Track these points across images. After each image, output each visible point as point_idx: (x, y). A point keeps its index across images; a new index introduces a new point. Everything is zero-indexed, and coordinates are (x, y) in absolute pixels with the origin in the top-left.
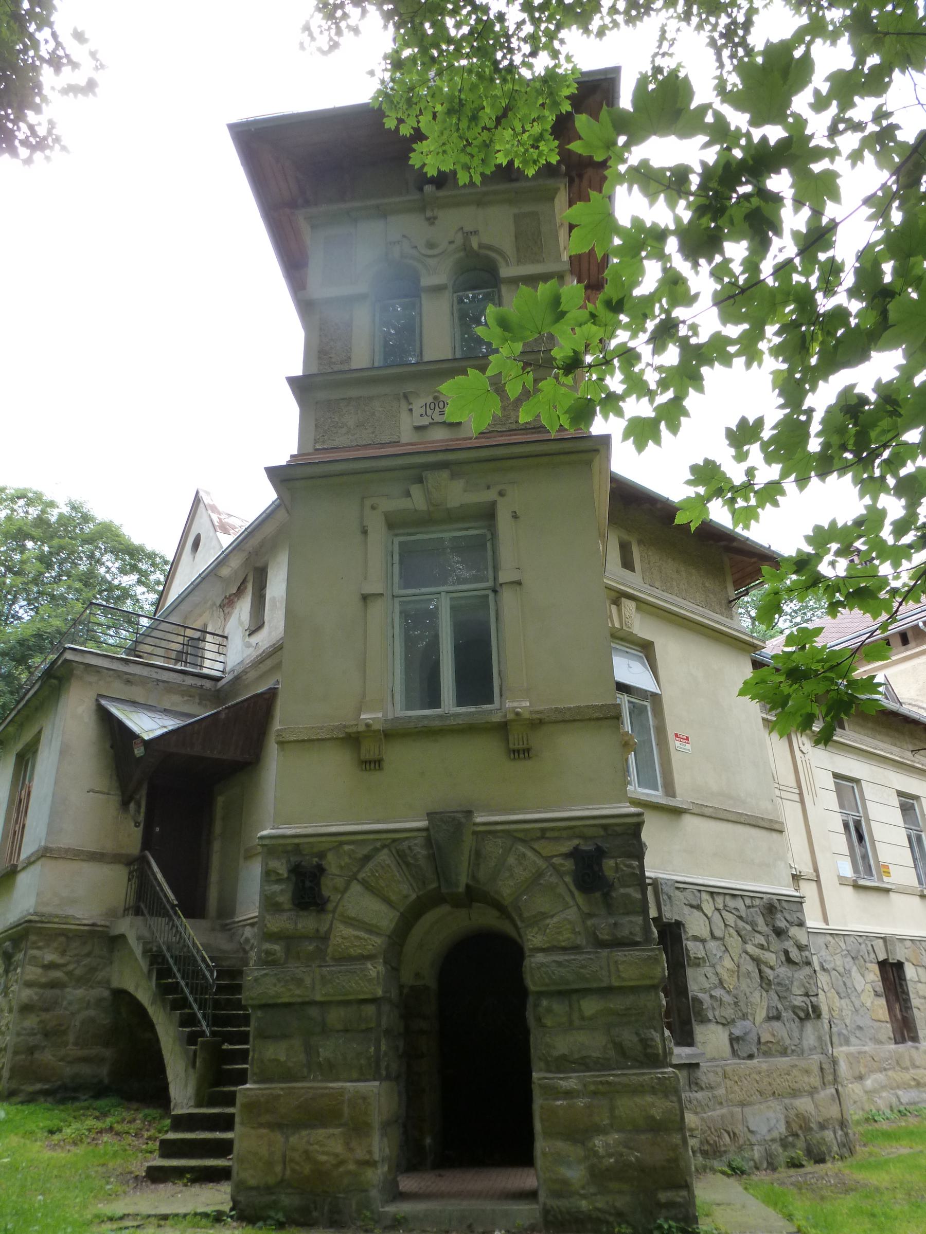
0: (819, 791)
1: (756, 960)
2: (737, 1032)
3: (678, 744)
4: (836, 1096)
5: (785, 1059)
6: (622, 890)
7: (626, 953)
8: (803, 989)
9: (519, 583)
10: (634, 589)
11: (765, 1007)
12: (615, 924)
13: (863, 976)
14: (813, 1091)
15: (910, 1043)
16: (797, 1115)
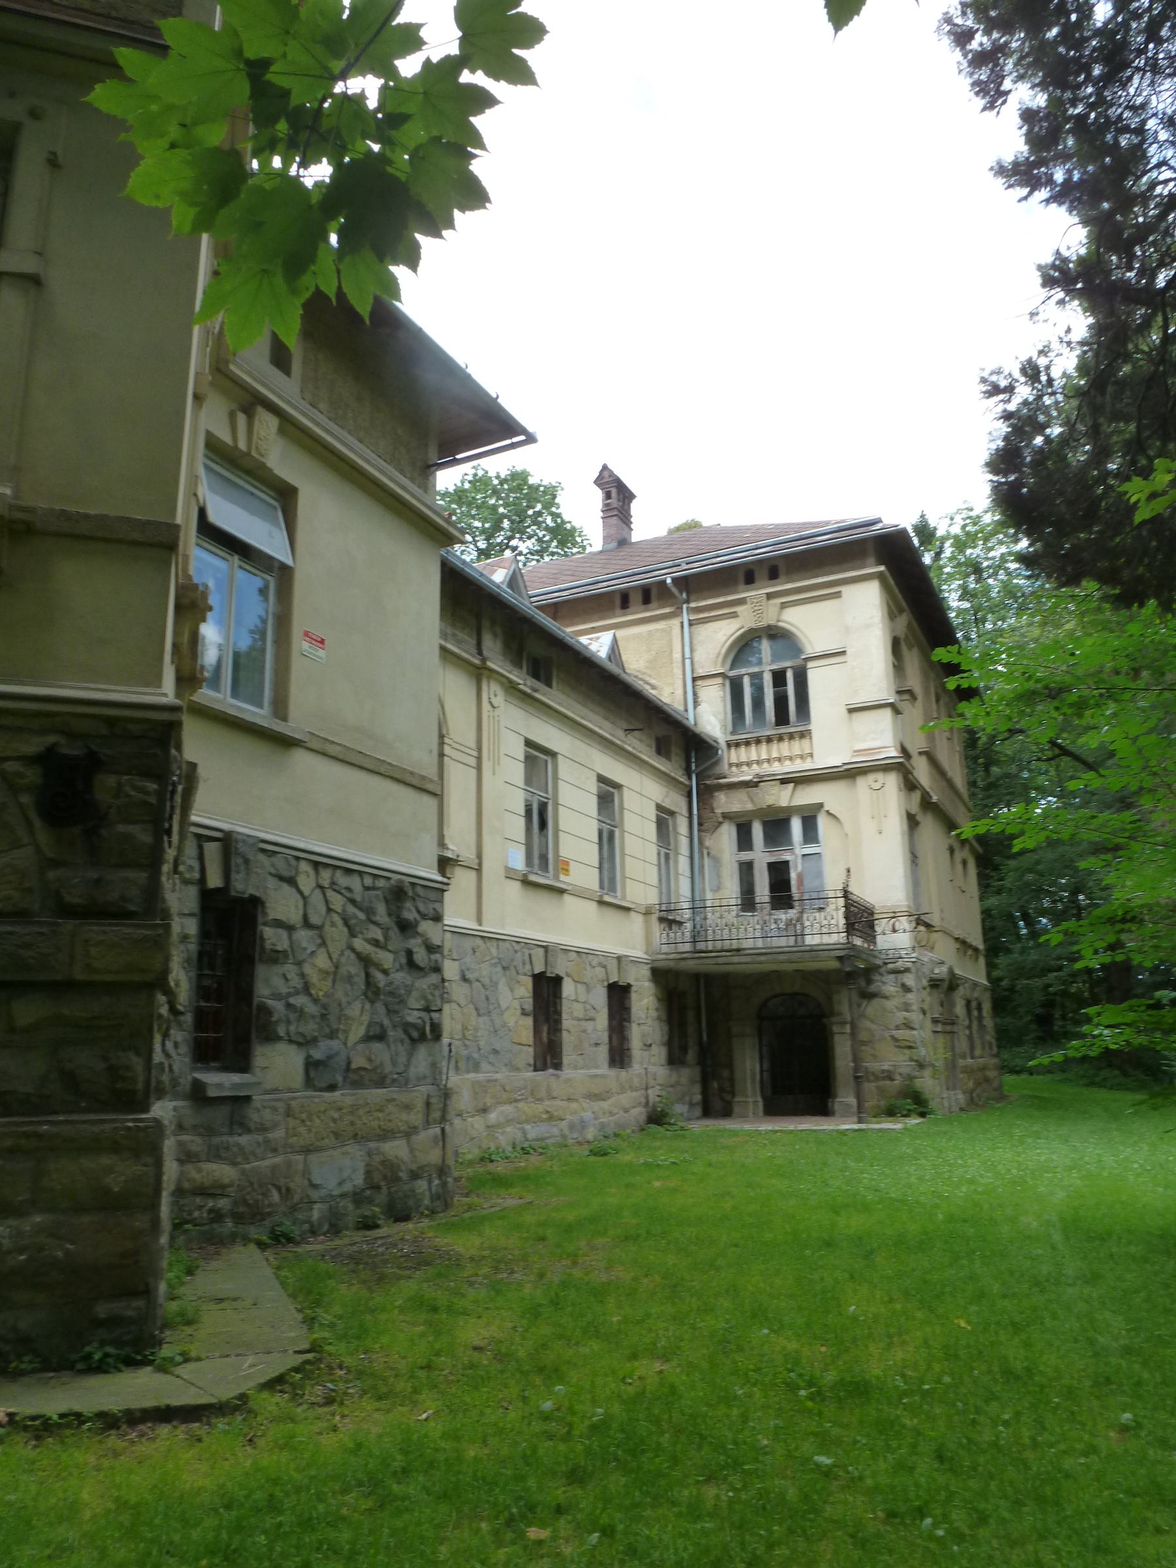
0: (504, 760)
1: (366, 961)
2: (317, 1054)
3: (306, 645)
4: (440, 1137)
5: (379, 1091)
6: (121, 828)
7: (107, 929)
8: (423, 1002)
9: (34, 281)
10: (279, 396)
11: (366, 1023)
12: (98, 881)
13: (512, 990)
14: (410, 1132)
15: (551, 1071)
16: (383, 1163)
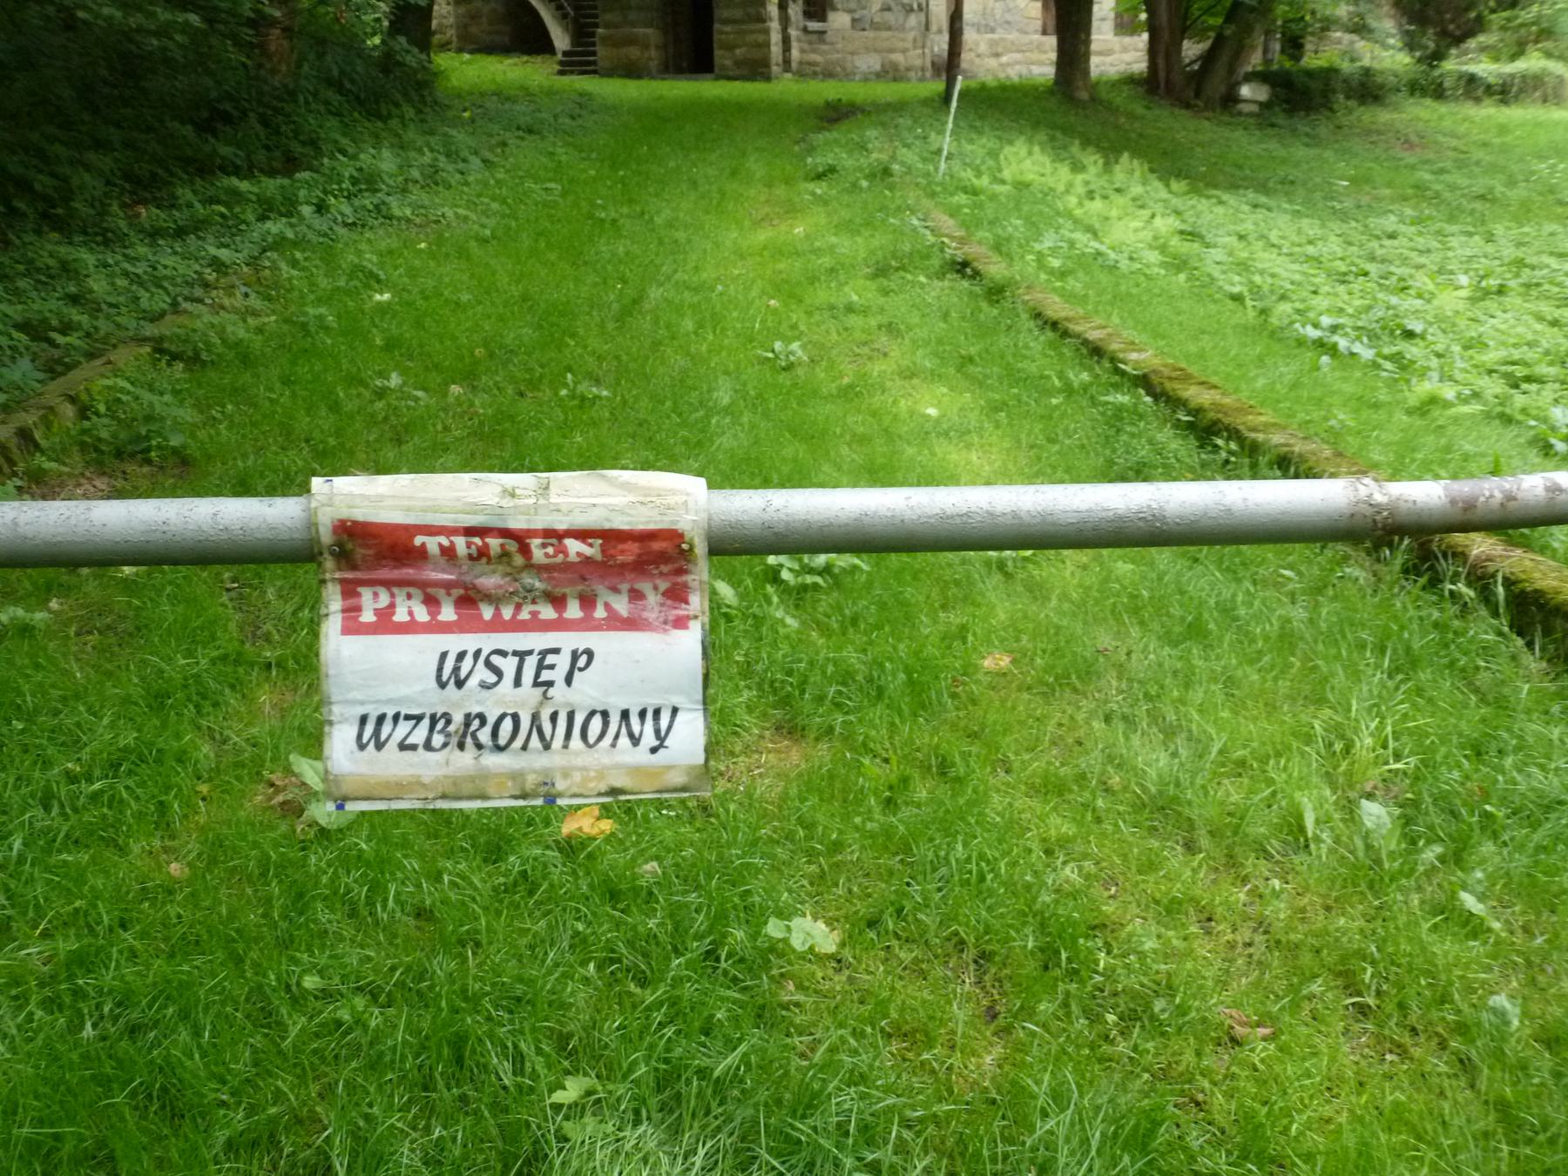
14: (904, 51)
